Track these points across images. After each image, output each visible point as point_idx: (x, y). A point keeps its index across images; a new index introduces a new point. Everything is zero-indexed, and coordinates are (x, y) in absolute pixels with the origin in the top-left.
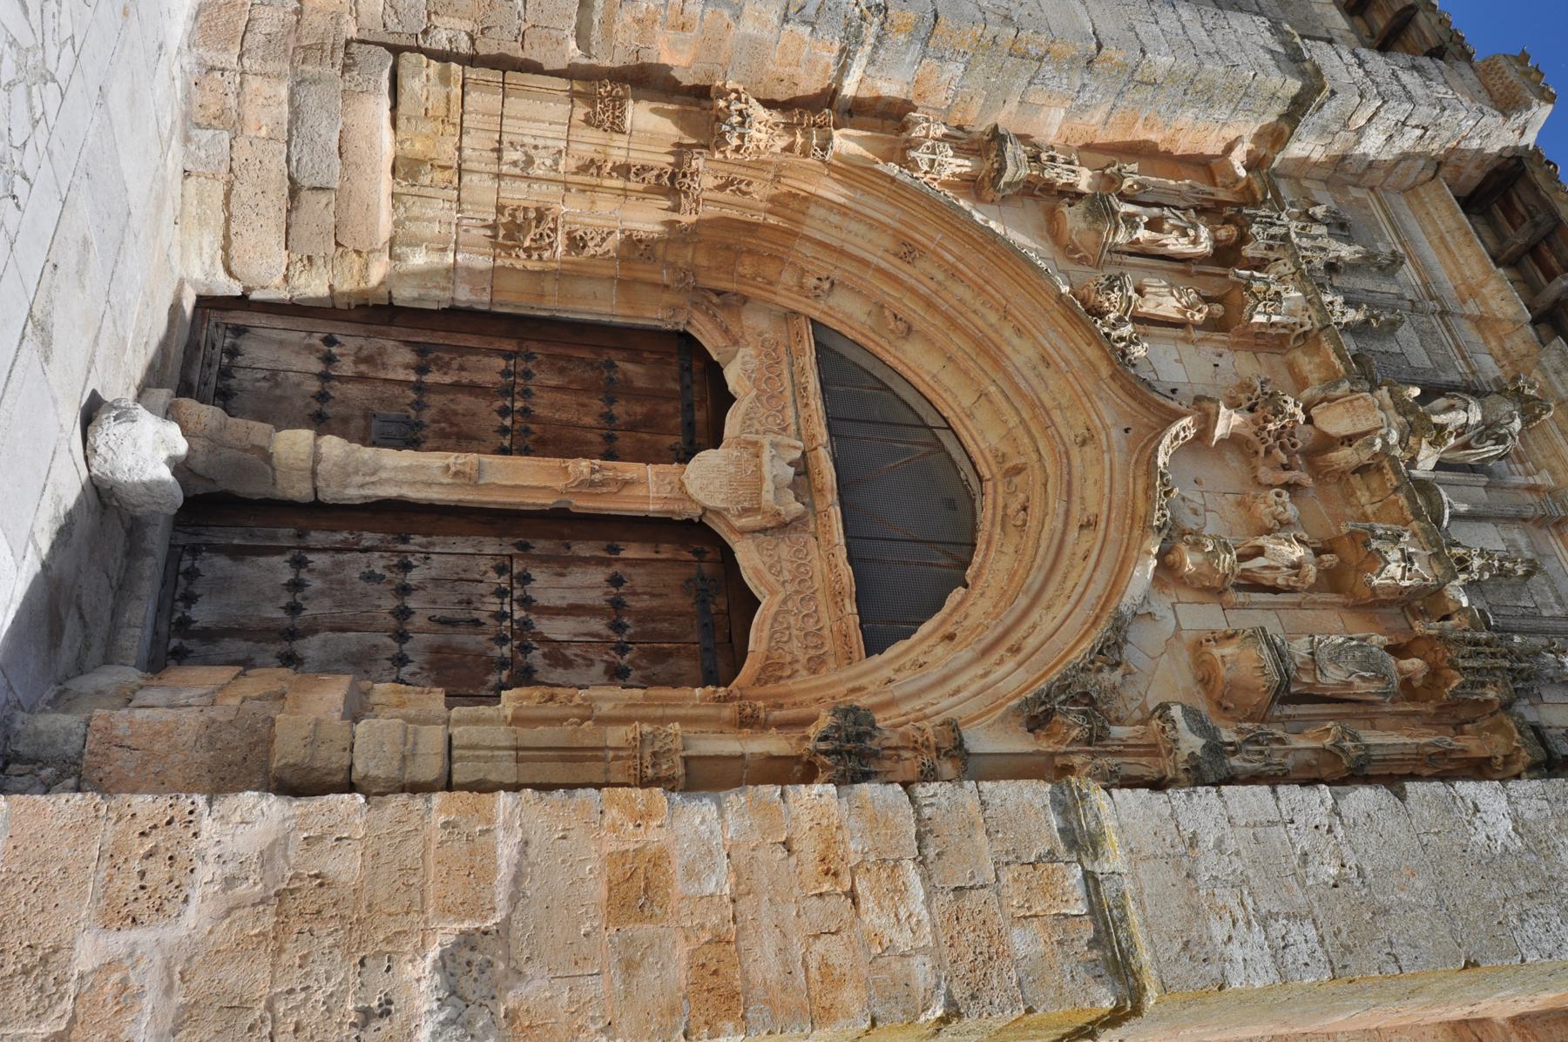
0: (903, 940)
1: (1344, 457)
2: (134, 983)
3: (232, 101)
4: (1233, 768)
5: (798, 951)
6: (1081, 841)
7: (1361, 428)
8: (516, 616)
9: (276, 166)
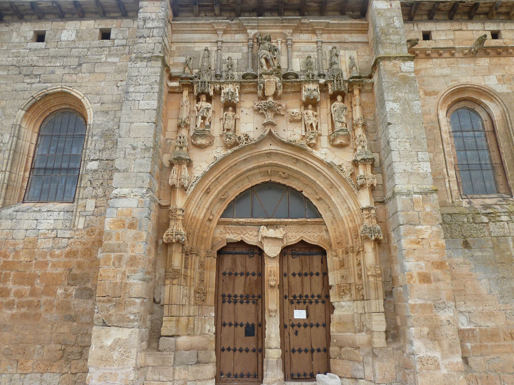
0: (430, 231)
1: (280, 92)
5: (432, 250)
8: (304, 298)
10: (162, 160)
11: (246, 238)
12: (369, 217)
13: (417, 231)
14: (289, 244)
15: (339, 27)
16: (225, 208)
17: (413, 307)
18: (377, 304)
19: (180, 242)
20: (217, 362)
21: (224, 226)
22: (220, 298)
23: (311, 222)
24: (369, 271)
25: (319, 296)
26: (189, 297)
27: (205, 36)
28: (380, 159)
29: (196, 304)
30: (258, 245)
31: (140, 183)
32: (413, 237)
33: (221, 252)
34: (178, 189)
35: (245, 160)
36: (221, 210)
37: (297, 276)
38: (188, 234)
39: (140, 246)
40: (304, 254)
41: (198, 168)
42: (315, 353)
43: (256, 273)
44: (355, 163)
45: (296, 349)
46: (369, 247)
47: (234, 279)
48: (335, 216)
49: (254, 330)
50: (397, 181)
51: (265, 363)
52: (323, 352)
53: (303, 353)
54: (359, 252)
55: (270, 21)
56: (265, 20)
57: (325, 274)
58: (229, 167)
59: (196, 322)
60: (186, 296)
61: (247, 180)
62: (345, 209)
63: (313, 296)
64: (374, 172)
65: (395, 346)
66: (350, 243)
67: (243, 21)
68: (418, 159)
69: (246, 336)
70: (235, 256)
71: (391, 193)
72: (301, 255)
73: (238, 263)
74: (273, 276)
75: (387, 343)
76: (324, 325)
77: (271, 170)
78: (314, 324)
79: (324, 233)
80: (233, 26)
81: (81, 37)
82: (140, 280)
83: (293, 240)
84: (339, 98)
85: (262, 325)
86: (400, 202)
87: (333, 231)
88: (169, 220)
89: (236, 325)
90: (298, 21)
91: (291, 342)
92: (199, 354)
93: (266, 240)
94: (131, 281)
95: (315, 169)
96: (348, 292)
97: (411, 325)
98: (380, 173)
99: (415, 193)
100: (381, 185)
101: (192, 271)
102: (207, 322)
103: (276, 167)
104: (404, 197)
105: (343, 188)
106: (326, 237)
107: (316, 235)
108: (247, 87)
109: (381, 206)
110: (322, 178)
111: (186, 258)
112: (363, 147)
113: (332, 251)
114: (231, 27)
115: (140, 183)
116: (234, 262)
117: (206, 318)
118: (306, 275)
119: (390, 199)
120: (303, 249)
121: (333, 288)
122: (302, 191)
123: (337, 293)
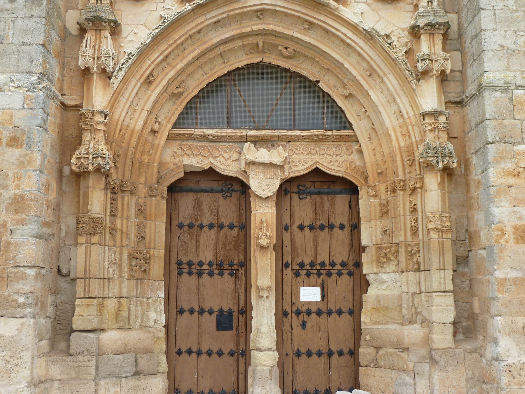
4: (438, 5)
8: (319, 268)
10: (64, 22)
11: (218, 165)
12: (435, 128)
13: (516, 155)
14: (293, 175)
16: (180, 110)
17: (502, 282)
18: (442, 278)
19: (102, 170)
20: (169, 373)
21: (179, 142)
22: (174, 267)
23: (333, 136)
24: (431, 221)
25: (343, 264)
26: (120, 266)
28: (459, 24)
29: (131, 277)
30: (240, 177)
31: (25, 64)
32: (509, 165)
33: (174, 189)
34: (95, 77)
35: (216, 23)
36: (173, 113)
37: (307, 230)
38: (116, 157)
39: (30, 177)
40: (320, 193)
41: (130, 38)
42: (335, 357)
43: (236, 224)
44: (415, 32)
45: (303, 350)
46: (432, 181)
48: (376, 127)
49: (232, 320)
50: (487, 66)
51: (250, 374)
52: (348, 356)
53: (314, 357)
54: (414, 189)
57: (356, 227)
58: (187, 36)
59: (132, 308)
60: (115, 263)
61: (221, 61)
62: (394, 114)
63: (333, 264)
64: (447, 47)
65: (467, 346)
66: (400, 173)
69: (218, 330)
70: (199, 195)
71: (476, 87)
72: (315, 194)
73: (205, 208)
74: (264, 230)
75: (456, 341)
76: (351, 313)
77: (264, 43)
78: (334, 310)
79: (355, 157)
82: (33, 236)
83: (300, 167)
85: (245, 311)
86: (491, 102)
87: (371, 151)
88: (81, 131)
89: (201, 312)
91: (295, 340)
92: (139, 360)
94: (17, 238)
95: (342, 40)
96: (393, 258)
97: (496, 313)
98: (458, 50)
99: (517, 87)
100: (459, 71)
101: (125, 221)
102: (151, 307)
103: (274, 38)
104: (498, 94)
105: (391, 76)
106: (358, 163)
107: (341, 159)
109: (458, 109)
110: (354, 58)
111: (113, 199)
113: (369, 187)
115: (25, 64)
116: (198, 205)
117: (150, 300)
119: (473, 97)
120: (318, 183)
121: (367, 250)
122: (318, 82)
123: (374, 258)
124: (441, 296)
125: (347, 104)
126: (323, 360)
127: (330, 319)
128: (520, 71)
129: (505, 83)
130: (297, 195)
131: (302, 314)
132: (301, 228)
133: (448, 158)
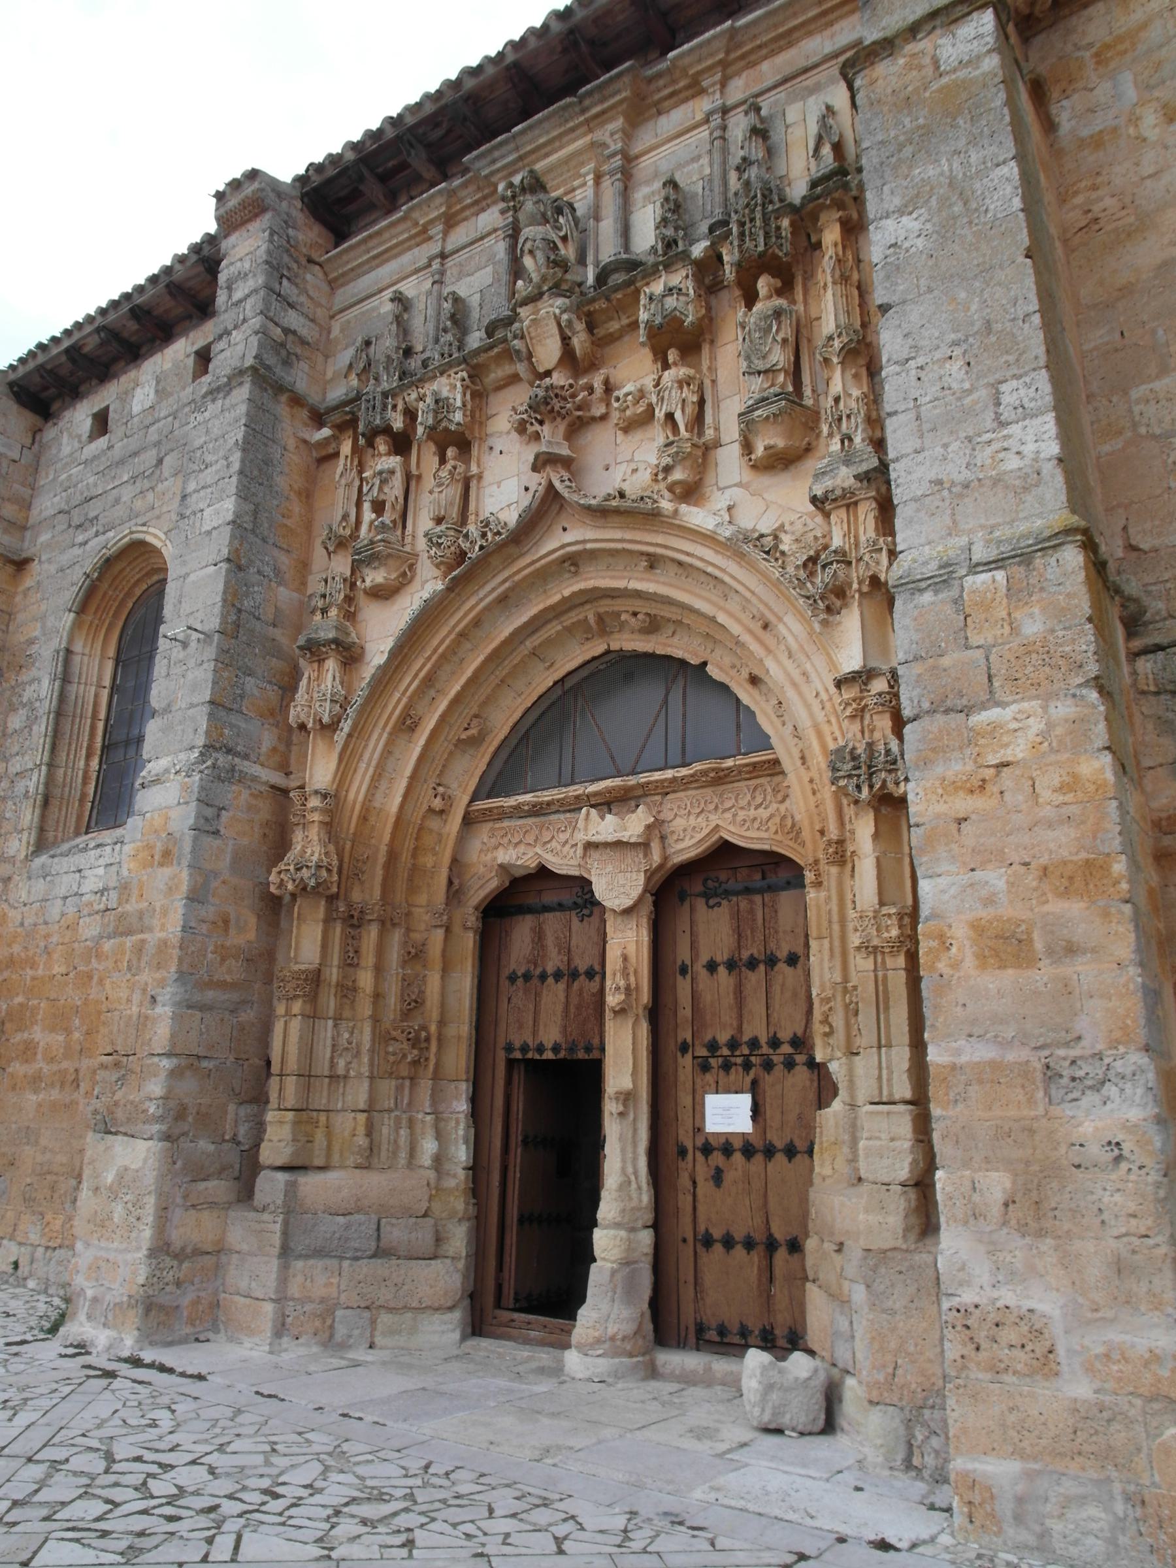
0: (1035, 725)
1: (579, 342)
2: (1100, 1350)
3: (308, 1307)
4: (863, 440)
5: (1047, 812)
6: (944, 577)
7: (555, 331)
8: (746, 1051)
9: (366, 1268)
13: (973, 738)
15: (776, 26)
16: (482, 766)
27: (406, 258)
32: (957, 767)
37: (722, 970)
40: (748, 891)
45: (717, 1233)
47: (538, 995)
53: (739, 1251)
55: (546, 125)
56: (530, 128)
61: (541, 666)
63: (775, 1043)
67: (478, 165)
68: (998, 415)
72: (737, 893)
73: (550, 941)
78: (779, 1144)
80: (463, 193)
81: (164, 389)
83: (687, 843)
84: (763, 284)
87: (808, 787)
90: (626, 79)
91: (701, 1208)
93: (595, 854)
99: (975, 568)
103: (608, 601)
104: (927, 597)
105: (790, 619)
108: (493, 366)
112: (847, 438)
114: (460, 201)
116: (539, 936)
118: (752, 964)
120: (724, 871)
122: (705, 664)
124: (878, 1113)
125: (758, 697)
126: (756, 1259)
127: (770, 1166)
128: (982, 527)
129: (941, 567)
130: (703, 900)
131: (715, 1153)
132: (712, 967)
133: (883, 775)
